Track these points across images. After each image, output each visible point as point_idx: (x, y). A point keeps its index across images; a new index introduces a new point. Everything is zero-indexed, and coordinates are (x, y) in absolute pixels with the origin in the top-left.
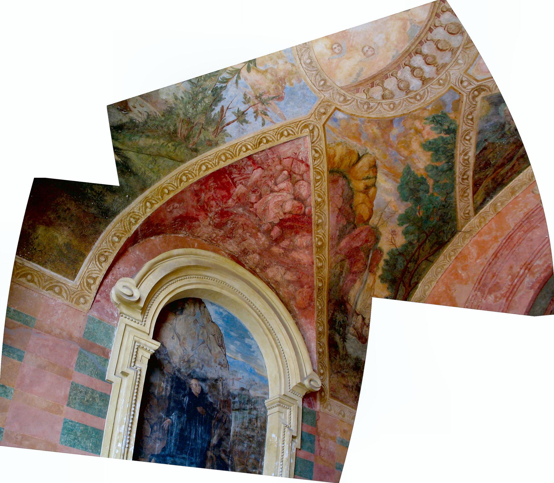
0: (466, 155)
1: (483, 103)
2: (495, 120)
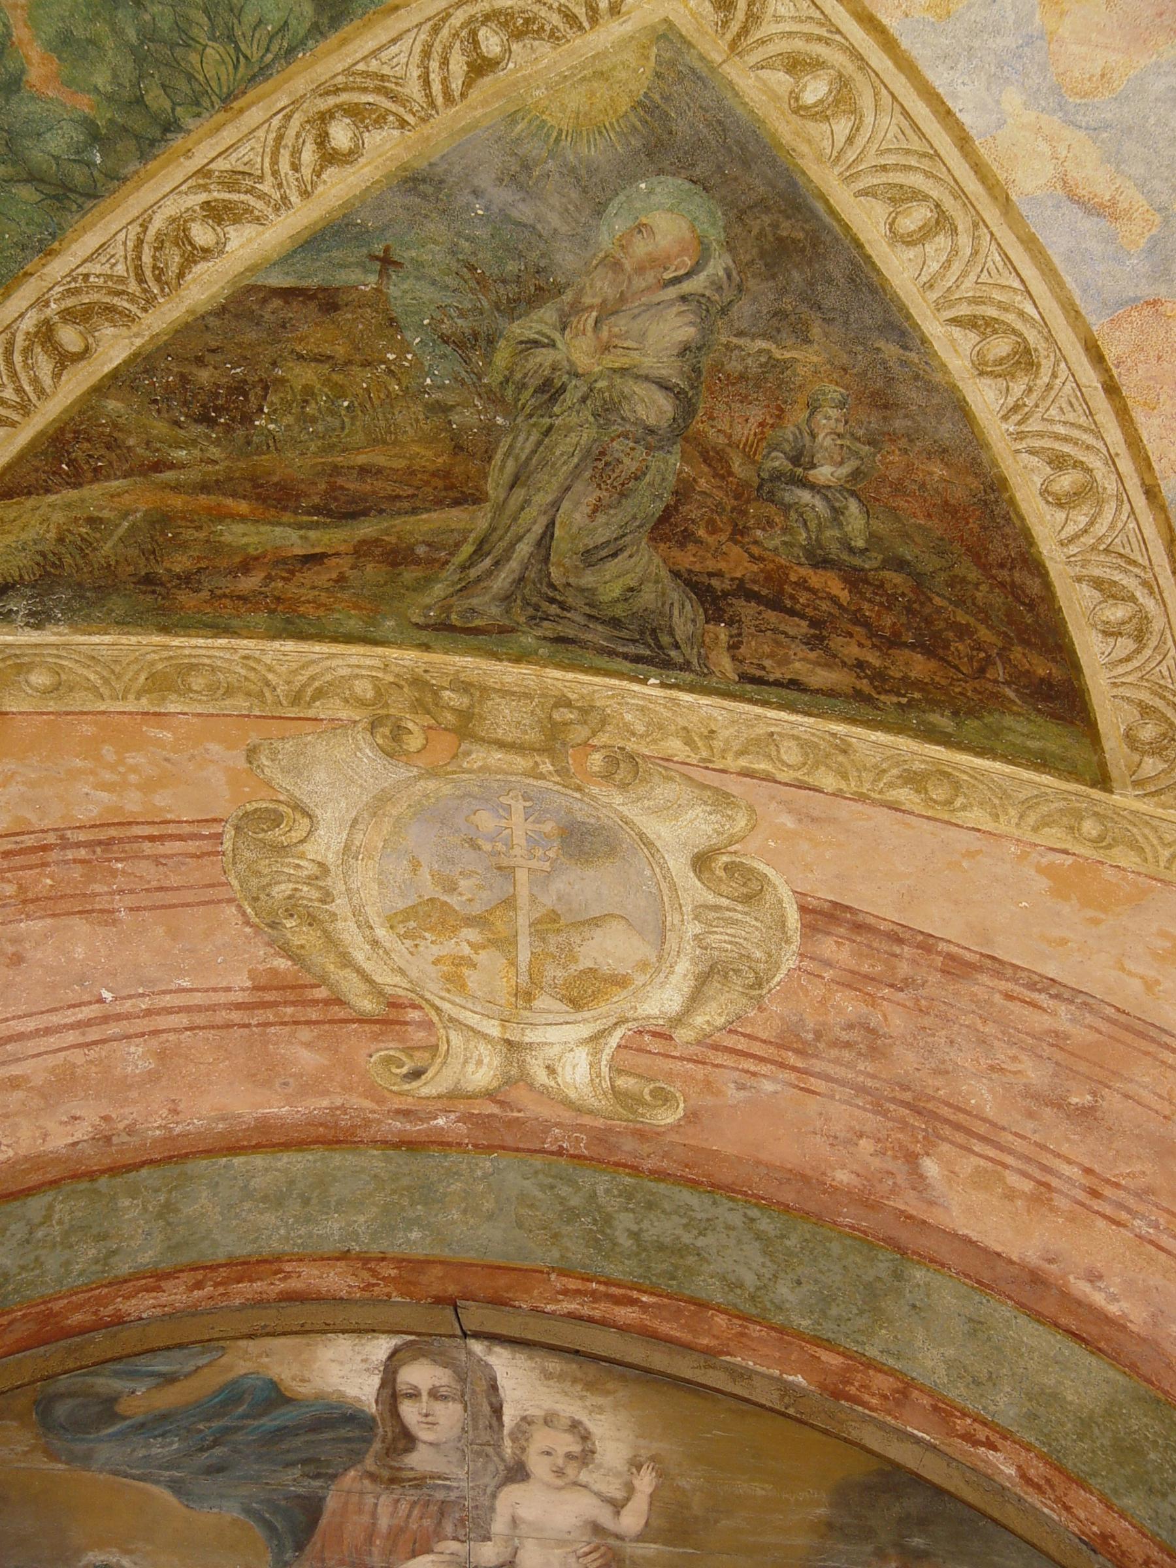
0: (216, 213)
1: (630, 57)
2: (550, 213)
